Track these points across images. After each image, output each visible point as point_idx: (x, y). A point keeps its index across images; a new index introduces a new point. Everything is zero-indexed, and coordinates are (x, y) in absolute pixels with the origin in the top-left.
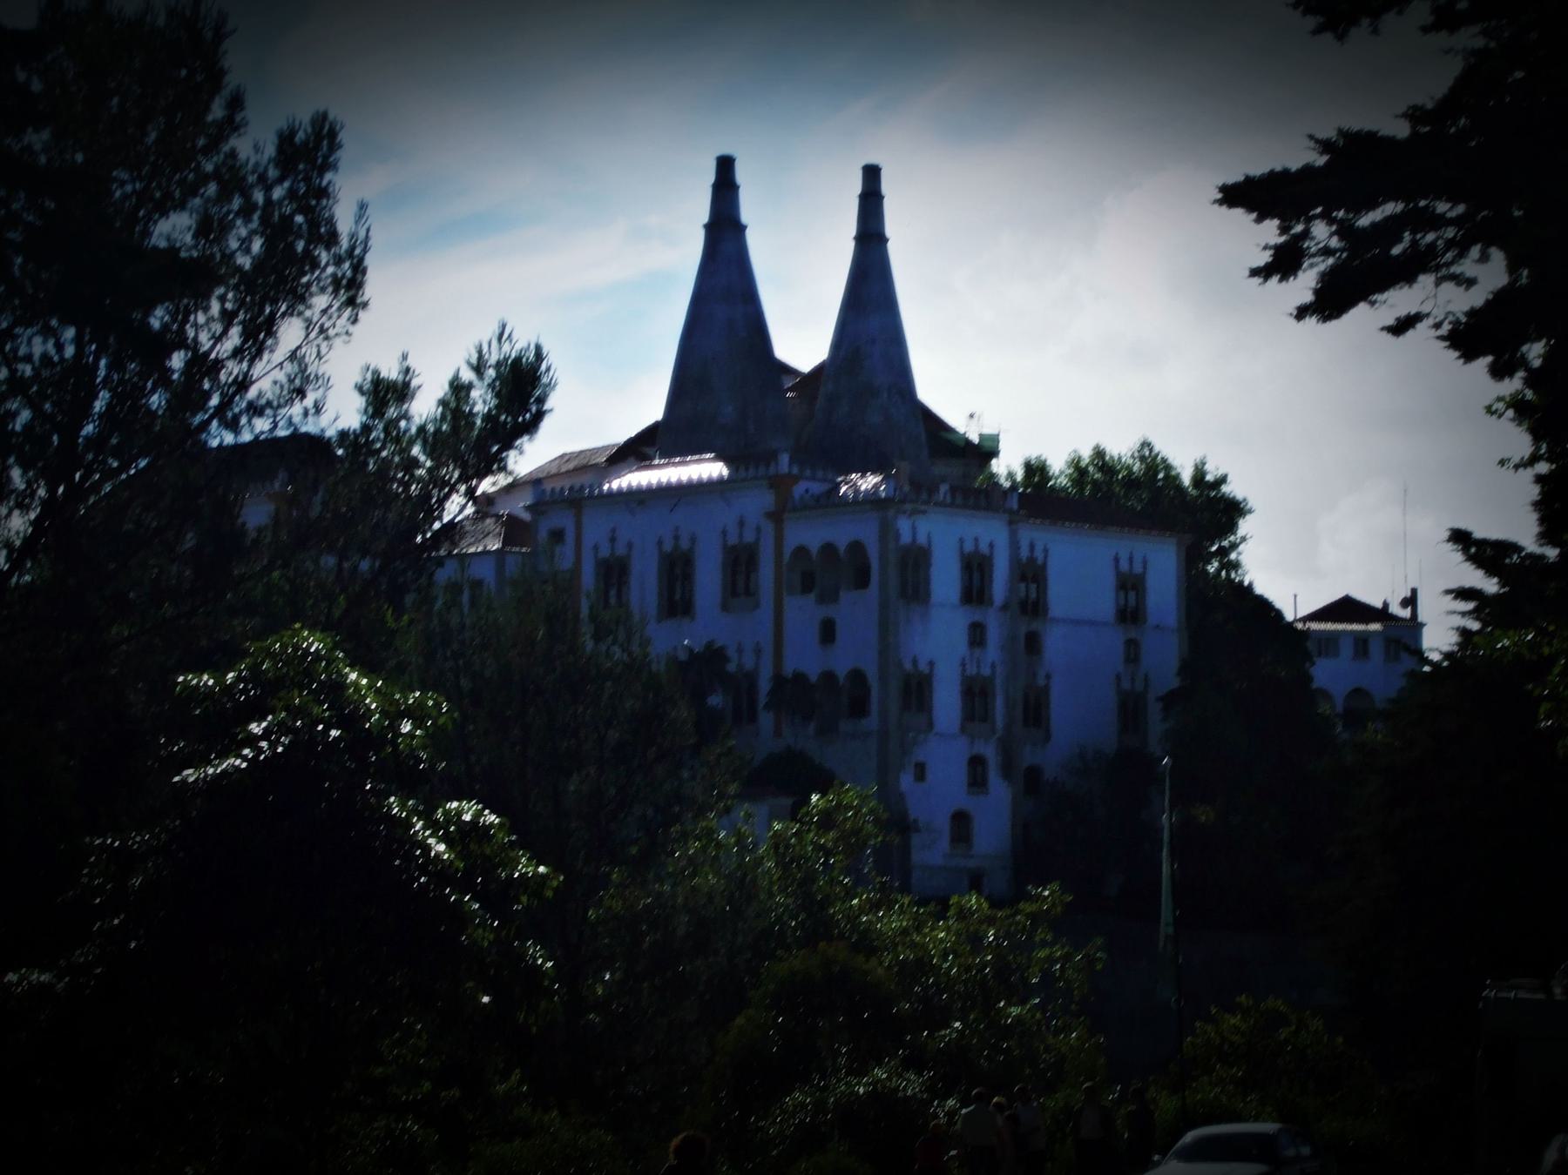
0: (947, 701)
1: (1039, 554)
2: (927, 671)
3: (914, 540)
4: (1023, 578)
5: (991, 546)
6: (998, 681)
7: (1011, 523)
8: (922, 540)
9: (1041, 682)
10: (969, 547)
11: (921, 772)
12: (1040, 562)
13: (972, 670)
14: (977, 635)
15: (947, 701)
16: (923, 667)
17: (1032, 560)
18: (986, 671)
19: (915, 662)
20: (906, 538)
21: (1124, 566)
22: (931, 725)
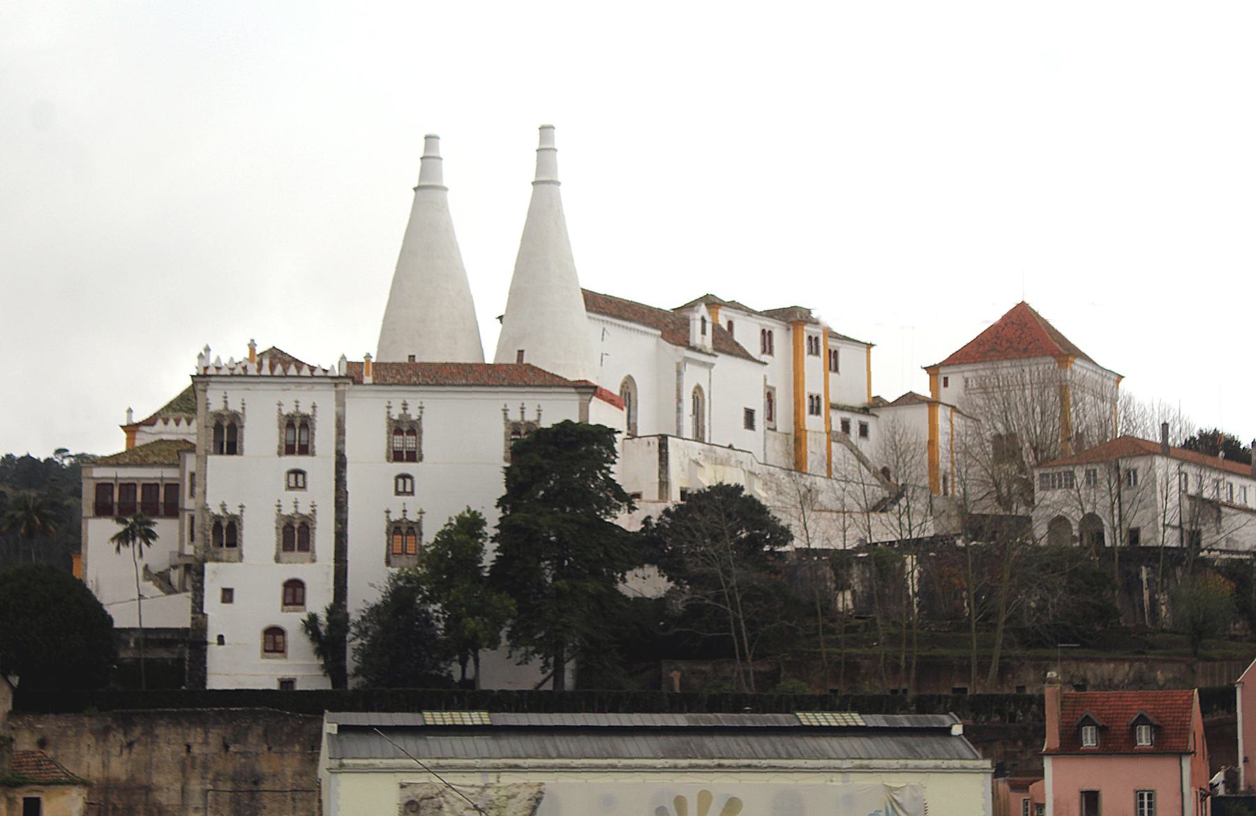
0: (260, 536)
1: (414, 414)
2: (237, 512)
3: (226, 408)
4: (398, 431)
5: (314, 407)
6: (319, 518)
7: (336, 385)
8: (235, 406)
9: (412, 517)
10: (288, 409)
11: (227, 596)
12: (414, 417)
13: (288, 510)
14: (297, 479)
15: (260, 536)
16: (233, 510)
17: (404, 417)
18: (305, 510)
19: (223, 506)
20: (216, 405)
21: (515, 416)
22: (240, 558)
